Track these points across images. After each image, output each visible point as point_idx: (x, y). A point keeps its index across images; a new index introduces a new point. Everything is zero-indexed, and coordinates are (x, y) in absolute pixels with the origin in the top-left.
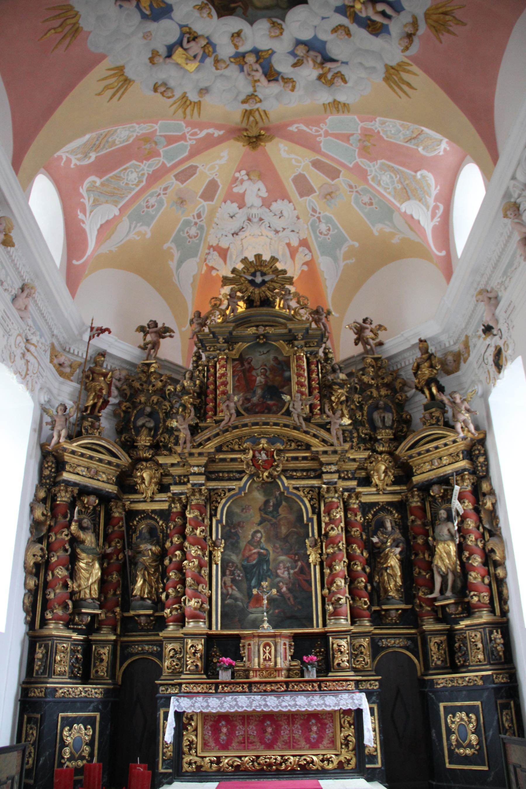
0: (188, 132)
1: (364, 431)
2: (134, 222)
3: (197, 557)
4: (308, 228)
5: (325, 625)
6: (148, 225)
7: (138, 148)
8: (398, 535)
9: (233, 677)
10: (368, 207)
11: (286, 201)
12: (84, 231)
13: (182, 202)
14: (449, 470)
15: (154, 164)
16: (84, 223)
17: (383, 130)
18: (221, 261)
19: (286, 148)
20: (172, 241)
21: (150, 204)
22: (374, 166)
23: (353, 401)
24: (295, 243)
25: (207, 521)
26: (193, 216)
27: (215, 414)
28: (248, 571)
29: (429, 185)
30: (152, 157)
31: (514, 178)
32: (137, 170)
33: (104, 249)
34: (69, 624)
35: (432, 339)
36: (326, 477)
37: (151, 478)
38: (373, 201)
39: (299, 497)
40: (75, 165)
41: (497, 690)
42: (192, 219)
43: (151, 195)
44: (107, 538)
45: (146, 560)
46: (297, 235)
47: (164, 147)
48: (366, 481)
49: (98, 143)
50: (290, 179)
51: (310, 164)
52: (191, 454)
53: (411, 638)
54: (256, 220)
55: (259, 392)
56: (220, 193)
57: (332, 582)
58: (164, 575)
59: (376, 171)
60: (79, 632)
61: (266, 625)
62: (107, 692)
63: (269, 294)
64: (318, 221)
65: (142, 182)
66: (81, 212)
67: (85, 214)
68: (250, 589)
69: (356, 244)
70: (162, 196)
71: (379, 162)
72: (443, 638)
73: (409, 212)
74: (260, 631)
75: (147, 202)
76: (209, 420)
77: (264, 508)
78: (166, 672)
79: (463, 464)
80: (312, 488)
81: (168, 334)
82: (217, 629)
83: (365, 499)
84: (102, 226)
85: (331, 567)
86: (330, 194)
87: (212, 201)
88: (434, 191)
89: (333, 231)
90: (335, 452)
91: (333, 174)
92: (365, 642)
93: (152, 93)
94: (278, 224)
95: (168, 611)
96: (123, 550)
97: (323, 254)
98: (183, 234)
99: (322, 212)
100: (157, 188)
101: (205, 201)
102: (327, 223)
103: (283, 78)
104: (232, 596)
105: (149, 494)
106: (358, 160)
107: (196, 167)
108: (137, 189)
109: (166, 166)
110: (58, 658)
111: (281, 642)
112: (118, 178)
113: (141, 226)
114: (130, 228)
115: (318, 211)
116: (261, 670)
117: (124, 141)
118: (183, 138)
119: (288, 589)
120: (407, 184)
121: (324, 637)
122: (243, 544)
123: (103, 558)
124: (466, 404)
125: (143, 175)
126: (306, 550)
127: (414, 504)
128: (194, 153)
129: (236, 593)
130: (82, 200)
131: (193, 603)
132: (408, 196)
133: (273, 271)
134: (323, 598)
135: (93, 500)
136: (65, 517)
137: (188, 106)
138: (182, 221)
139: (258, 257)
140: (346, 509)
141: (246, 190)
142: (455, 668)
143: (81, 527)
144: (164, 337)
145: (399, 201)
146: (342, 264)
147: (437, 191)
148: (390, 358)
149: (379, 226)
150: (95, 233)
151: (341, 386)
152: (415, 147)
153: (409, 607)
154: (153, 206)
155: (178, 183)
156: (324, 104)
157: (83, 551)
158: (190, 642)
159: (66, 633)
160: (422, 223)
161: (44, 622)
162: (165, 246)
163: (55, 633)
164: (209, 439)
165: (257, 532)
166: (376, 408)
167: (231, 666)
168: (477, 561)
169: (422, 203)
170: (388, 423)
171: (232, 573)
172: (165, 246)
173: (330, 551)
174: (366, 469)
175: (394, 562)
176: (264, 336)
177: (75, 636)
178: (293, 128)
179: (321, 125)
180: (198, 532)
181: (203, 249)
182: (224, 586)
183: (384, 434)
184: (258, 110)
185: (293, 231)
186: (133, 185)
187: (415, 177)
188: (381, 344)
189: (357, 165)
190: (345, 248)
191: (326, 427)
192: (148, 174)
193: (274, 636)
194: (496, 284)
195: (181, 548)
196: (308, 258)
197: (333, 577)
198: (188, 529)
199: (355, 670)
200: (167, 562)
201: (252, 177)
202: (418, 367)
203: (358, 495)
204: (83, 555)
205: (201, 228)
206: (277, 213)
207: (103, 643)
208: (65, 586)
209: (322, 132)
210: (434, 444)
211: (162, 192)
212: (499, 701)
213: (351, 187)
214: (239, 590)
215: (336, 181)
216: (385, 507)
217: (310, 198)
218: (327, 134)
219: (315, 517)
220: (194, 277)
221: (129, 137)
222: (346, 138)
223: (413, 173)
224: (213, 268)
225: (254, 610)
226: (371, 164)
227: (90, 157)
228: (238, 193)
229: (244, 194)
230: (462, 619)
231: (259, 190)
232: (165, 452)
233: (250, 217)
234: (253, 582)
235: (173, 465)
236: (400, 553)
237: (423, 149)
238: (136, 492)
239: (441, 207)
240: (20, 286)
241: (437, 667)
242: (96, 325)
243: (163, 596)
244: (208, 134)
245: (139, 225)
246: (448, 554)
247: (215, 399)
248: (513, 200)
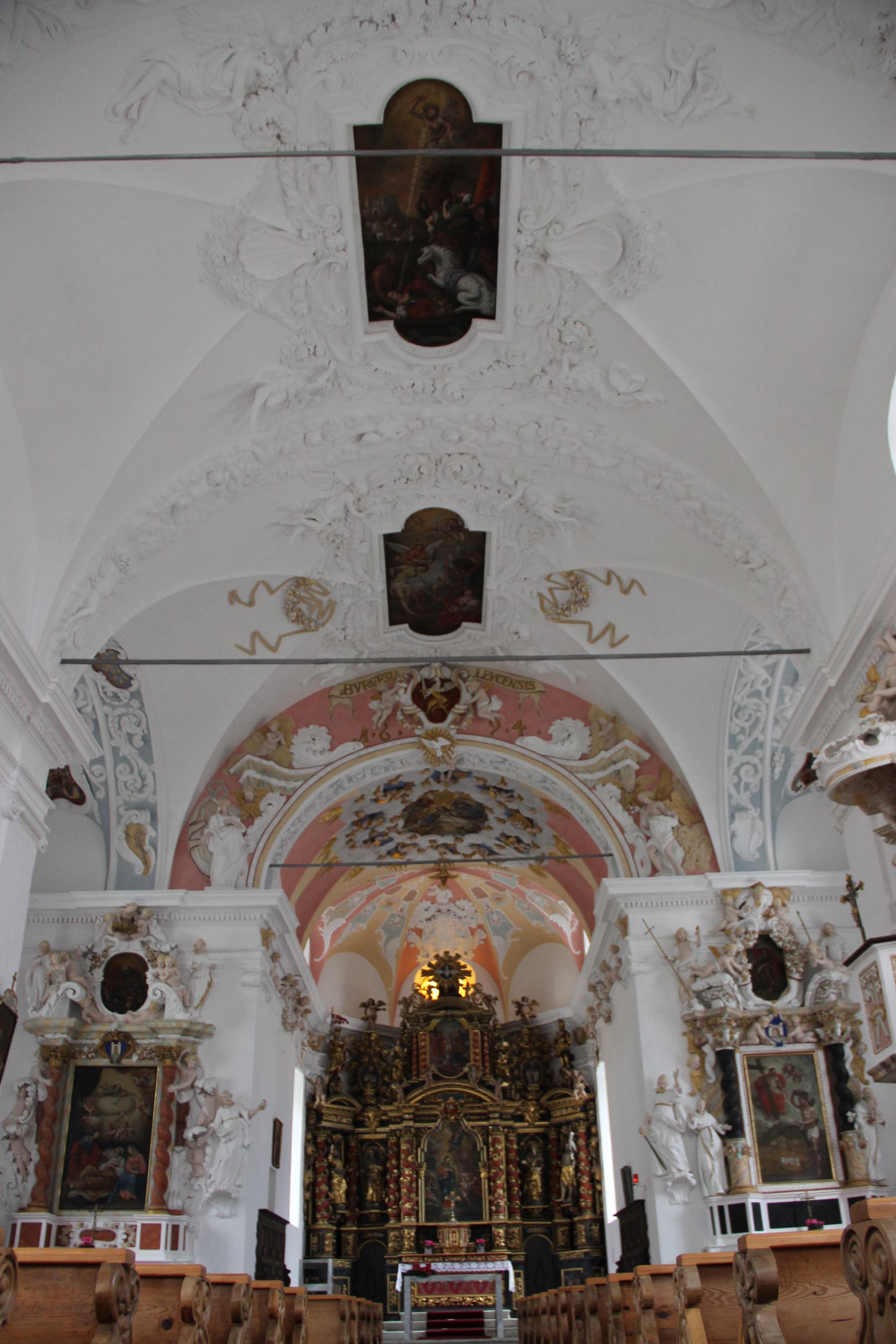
1: (519, 1084)
3: (410, 1175)
5: (490, 1219)
8: (540, 1158)
9: (433, 1252)
12: (322, 938)
13: (390, 904)
14: (572, 1117)
15: (372, 889)
18: (418, 937)
23: (512, 1063)
24: (474, 926)
25: (414, 1151)
27: (418, 1075)
28: (442, 1183)
33: (334, 945)
34: (330, 1220)
35: (568, 1019)
36: (492, 1121)
37: (375, 1117)
39: (474, 1133)
41: (593, 1261)
44: (347, 1162)
45: (374, 1175)
48: (521, 1119)
52: (404, 1107)
53: (547, 1227)
55: (448, 1056)
56: (418, 896)
57: (495, 1191)
58: (386, 1184)
60: (334, 1225)
61: (453, 1220)
62: (355, 1265)
63: (455, 984)
68: (443, 1195)
69: (520, 930)
72: (566, 1228)
73: (555, 921)
74: (449, 1223)
76: (414, 1078)
77: (451, 1141)
78: (390, 1250)
79: (582, 1115)
80: (483, 1127)
81: (382, 1007)
82: (422, 1222)
83: (520, 1131)
84: (334, 933)
85: (495, 1182)
86: (499, 899)
90: (498, 1105)
92: (516, 1230)
94: (460, 913)
95: (390, 1210)
96: (358, 1169)
100: (374, 901)
104: (431, 1200)
105: (373, 1127)
108: (359, 905)
110: (327, 1242)
111: (463, 1230)
115: (490, 905)
116: (450, 1248)
119: (468, 1195)
121: (489, 1227)
122: (438, 1165)
123: (347, 1176)
124: (581, 1077)
126: (479, 1169)
127: (552, 1137)
129: (435, 1199)
131: (407, 1205)
134: (491, 1203)
135: (340, 1136)
136: (323, 1150)
140: (507, 1140)
142: (574, 1247)
143: (335, 1157)
144: (379, 1010)
146: (510, 941)
148: (537, 1027)
150: (329, 938)
151: (504, 1053)
153: (546, 1206)
157: (336, 1172)
158: (406, 1231)
159: (330, 1227)
161: (315, 1220)
162: (376, 932)
163: (323, 1227)
164: (416, 1097)
165: (447, 1157)
166: (528, 1067)
167: (432, 1246)
168: (585, 1179)
170: (536, 1079)
171: (432, 1185)
172: (376, 932)
173: (494, 1171)
174: (520, 1110)
175: (536, 1177)
176: (452, 1016)
177: (334, 1228)
180: (410, 1158)
182: (427, 1193)
183: (533, 1087)
188: (533, 1016)
190: (512, 931)
191: (491, 1088)
193: (458, 1227)
195: (398, 1167)
196: (484, 937)
197: (497, 1187)
198: (403, 1156)
199: (509, 1248)
200: (388, 1177)
202: (556, 1041)
203: (513, 1129)
204: (336, 1175)
205: (403, 918)
207: (349, 1232)
208: (327, 1196)
210: (561, 1100)
212: (593, 1268)
214: (436, 1195)
216: (533, 1137)
219: (485, 1148)
220: (398, 951)
225: (445, 1209)
230: (575, 1216)
232: (384, 1100)
234: (445, 1191)
235: (390, 1111)
236: (541, 1171)
238: (364, 1126)
241: (562, 1247)
242: (336, 1013)
243: (387, 1200)
246: (569, 1173)
247: (418, 1062)
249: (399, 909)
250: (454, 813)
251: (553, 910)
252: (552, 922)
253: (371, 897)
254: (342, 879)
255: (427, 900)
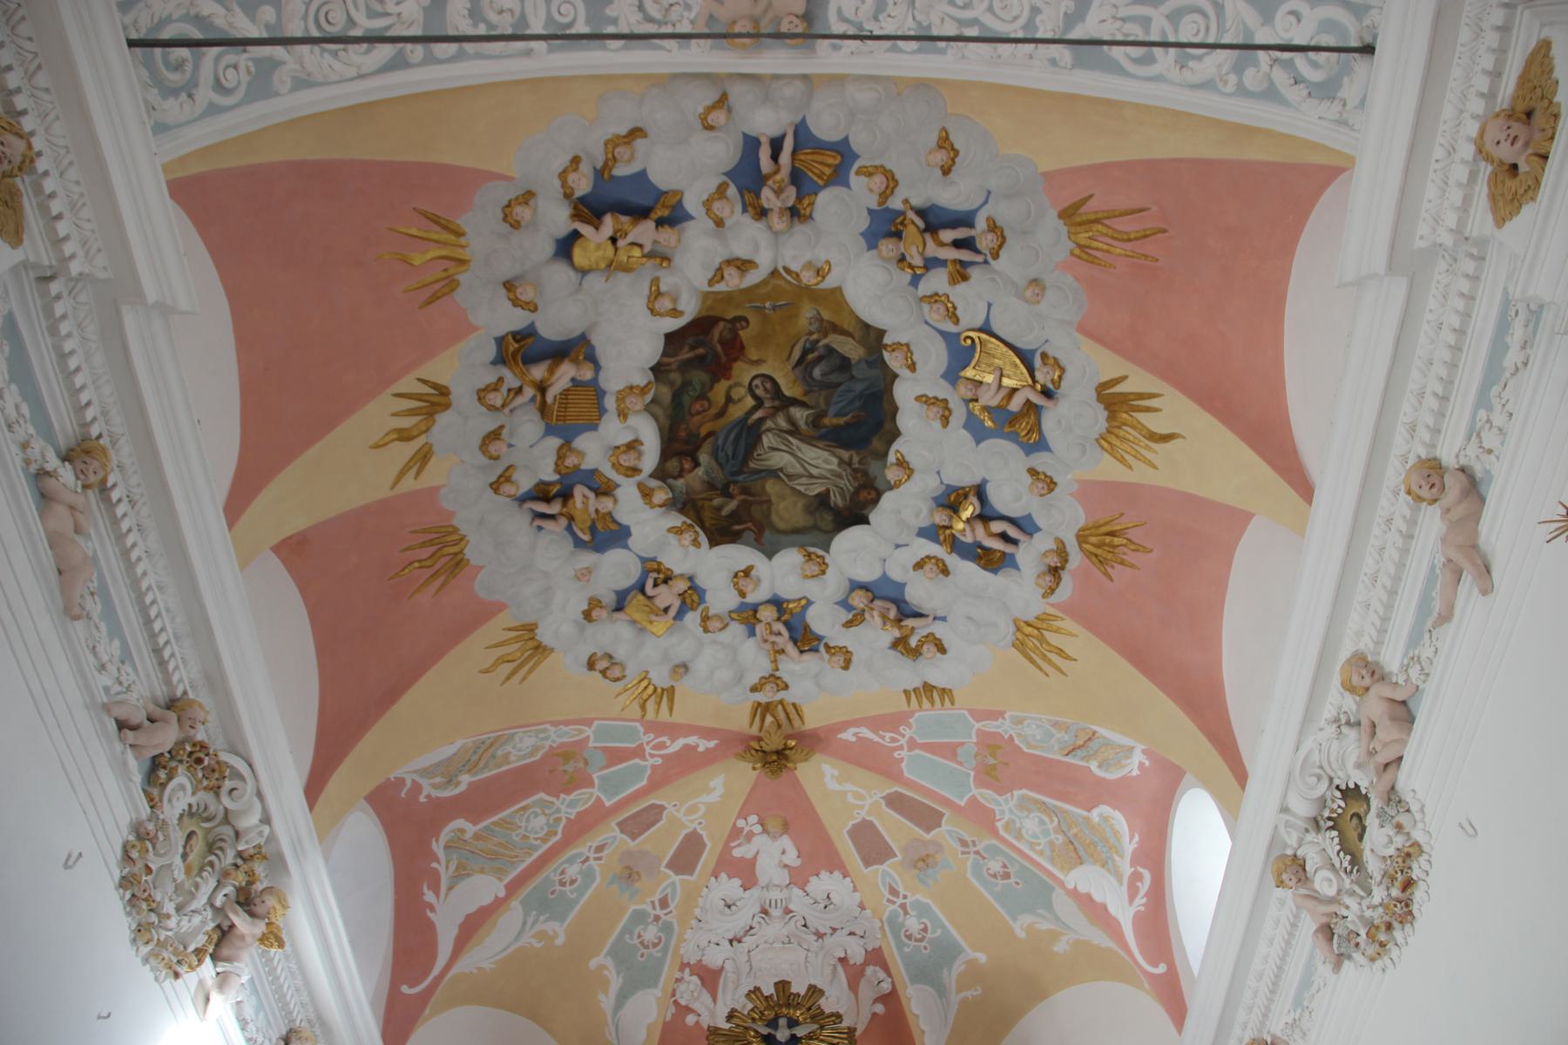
0: (648, 743)
2: (534, 913)
4: (882, 928)
6: (562, 920)
7: (551, 771)
10: (1001, 882)
11: (837, 874)
12: (431, 926)
13: (630, 875)
16: (432, 909)
17: (1019, 735)
18: (706, 997)
19: (836, 773)
20: (609, 953)
21: (567, 878)
22: (1007, 802)
24: (857, 956)
26: (653, 902)
29: (1116, 834)
30: (578, 787)
31: (1285, 809)
32: (547, 812)
38: (1010, 870)
40: (428, 796)
42: (649, 909)
43: (571, 861)
46: (862, 942)
47: (602, 769)
49: (475, 757)
50: (845, 831)
51: (883, 803)
54: (776, 913)
56: (707, 859)
59: (1011, 811)
64: (902, 912)
65: (555, 834)
66: (429, 889)
67: (437, 894)
69: (982, 958)
70: (592, 862)
71: (1016, 793)
73: (1082, 889)
75: (563, 872)
84: (468, 917)
87: (691, 874)
88: (1129, 845)
89: (934, 931)
91: (927, 818)
93: (585, 670)
97: (913, 982)
98: (631, 938)
99: (909, 894)
100: (584, 848)
101: (677, 874)
102: (919, 916)
103: (827, 646)
106: (975, 792)
107: (662, 808)
109: (603, 804)
112: (507, 824)
113: (547, 920)
114: (525, 923)
115: (902, 892)
117: (524, 757)
118: (639, 752)
120: (1075, 835)
125: (558, 820)
128: (660, 780)
130: (434, 865)
132: (1080, 858)
133: (813, 1017)
137: (650, 696)
138: (630, 911)
139: (782, 985)
141: (757, 853)
145: (1062, 869)
146: (955, 999)
147: (1134, 845)
149: (1026, 919)
150: (455, 931)
152: (1083, 763)
154: (573, 882)
155: (627, 839)
156: (906, 692)
160: (1112, 910)
169: (1109, 871)
178: (848, 735)
179: (901, 728)
181: (668, 971)
184: (781, 702)
185: (852, 934)
186: (536, 839)
187: (1087, 820)
189: (973, 800)
190: (958, 967)
192: (568, 819)
194: (1281, 1026)
196: (886, 987)
201: (770, 828)
205: (668, 928)
206: (819, 900)
209: (903, 741)
211: (592, 855)
213: (964, 843)
215: (934, 832)
217: (884, 867)
218: (912, 745)
220: (650, 1027)
221: (536, 749)
222: (949, 751)
223: (1085, 813)
224: (688, 1010)
226: (1000, 799)
227: (458, 784)
228: (742, 858)
229: (755, 858)
231: (783, 852)
233: (767, 907)
237: (1100, 767)
239: (1147, 875)
240: (284, 1032)
244: (686, 747)
245: (542, 918)
248: (1289, 852)
249: (656, 898)
250: (799, 414)
251: (1075, 851)
252: (1074, 894)
253: (580, 827)
254: (476, 648)
255: (730, 877)
